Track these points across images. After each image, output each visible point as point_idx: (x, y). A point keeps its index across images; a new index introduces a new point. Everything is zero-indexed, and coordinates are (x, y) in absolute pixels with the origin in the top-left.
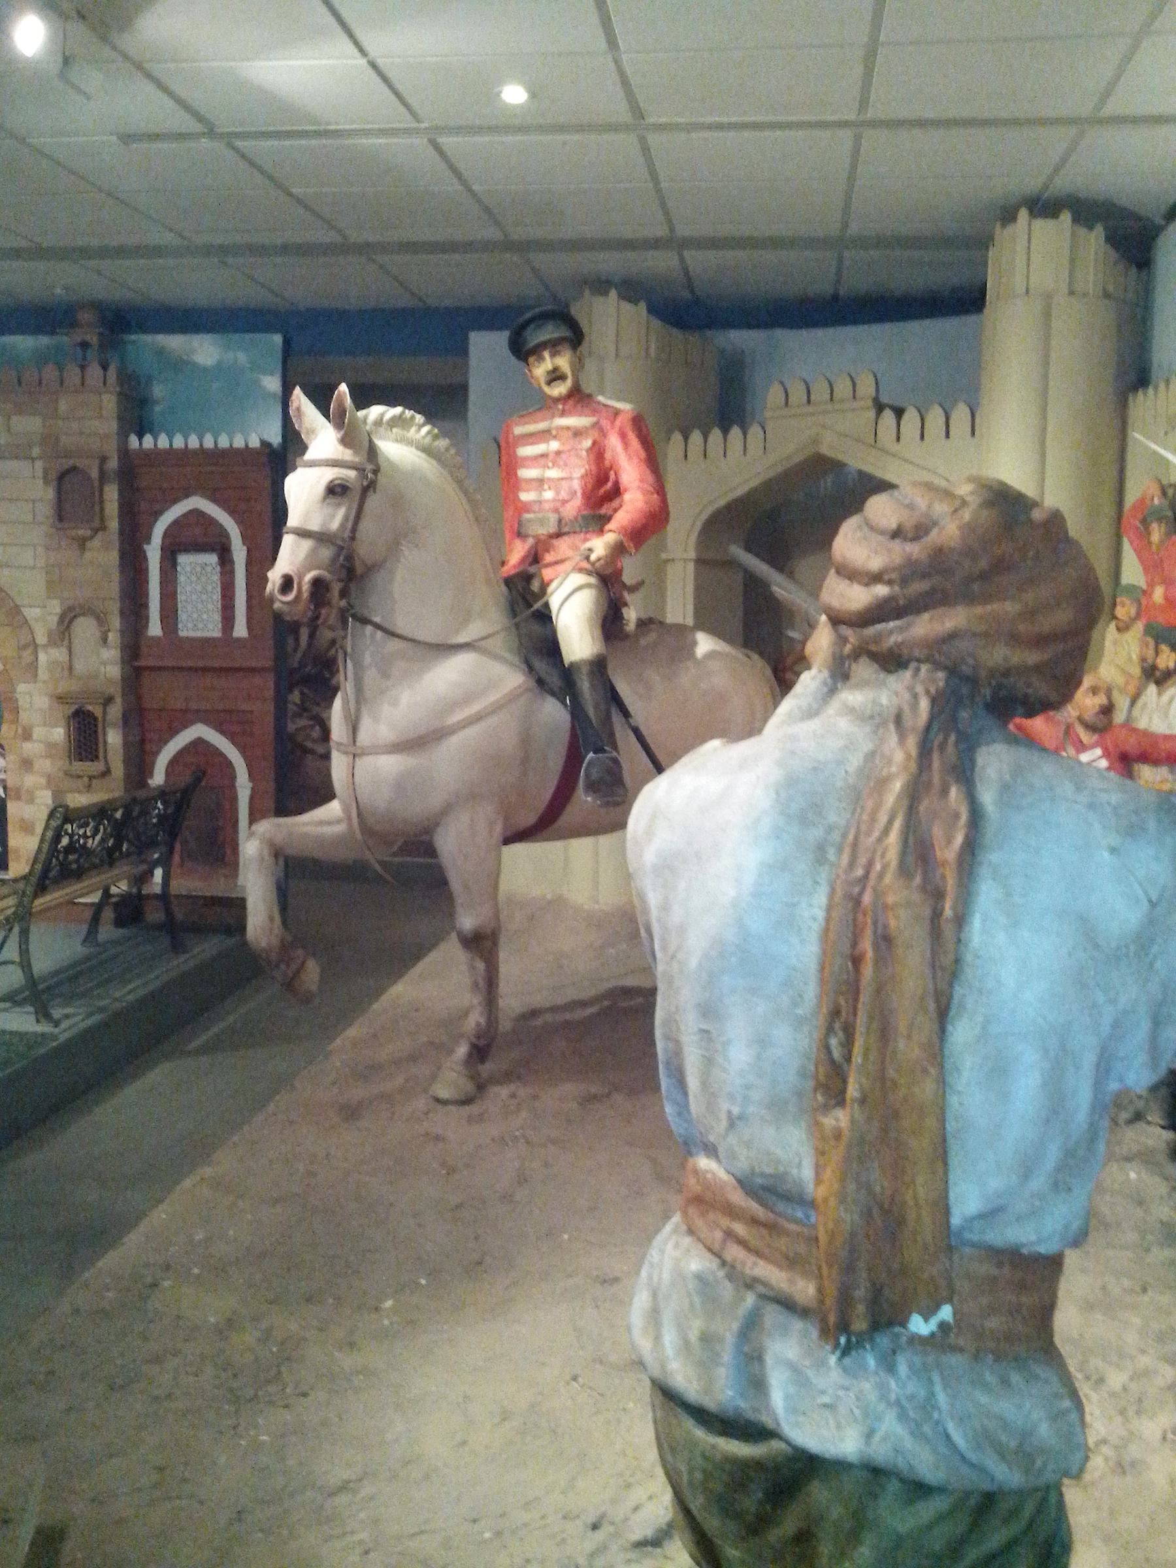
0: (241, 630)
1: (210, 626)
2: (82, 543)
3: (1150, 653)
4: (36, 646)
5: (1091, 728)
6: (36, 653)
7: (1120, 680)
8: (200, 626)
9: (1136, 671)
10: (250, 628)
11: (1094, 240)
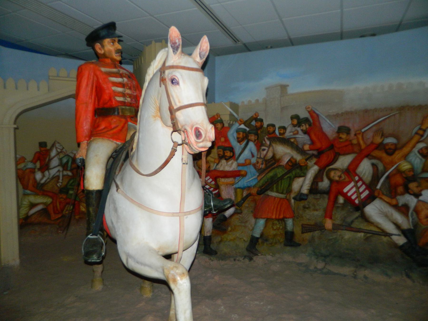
3: (221, 153)
7: (213, 160)
9: (217, 157)
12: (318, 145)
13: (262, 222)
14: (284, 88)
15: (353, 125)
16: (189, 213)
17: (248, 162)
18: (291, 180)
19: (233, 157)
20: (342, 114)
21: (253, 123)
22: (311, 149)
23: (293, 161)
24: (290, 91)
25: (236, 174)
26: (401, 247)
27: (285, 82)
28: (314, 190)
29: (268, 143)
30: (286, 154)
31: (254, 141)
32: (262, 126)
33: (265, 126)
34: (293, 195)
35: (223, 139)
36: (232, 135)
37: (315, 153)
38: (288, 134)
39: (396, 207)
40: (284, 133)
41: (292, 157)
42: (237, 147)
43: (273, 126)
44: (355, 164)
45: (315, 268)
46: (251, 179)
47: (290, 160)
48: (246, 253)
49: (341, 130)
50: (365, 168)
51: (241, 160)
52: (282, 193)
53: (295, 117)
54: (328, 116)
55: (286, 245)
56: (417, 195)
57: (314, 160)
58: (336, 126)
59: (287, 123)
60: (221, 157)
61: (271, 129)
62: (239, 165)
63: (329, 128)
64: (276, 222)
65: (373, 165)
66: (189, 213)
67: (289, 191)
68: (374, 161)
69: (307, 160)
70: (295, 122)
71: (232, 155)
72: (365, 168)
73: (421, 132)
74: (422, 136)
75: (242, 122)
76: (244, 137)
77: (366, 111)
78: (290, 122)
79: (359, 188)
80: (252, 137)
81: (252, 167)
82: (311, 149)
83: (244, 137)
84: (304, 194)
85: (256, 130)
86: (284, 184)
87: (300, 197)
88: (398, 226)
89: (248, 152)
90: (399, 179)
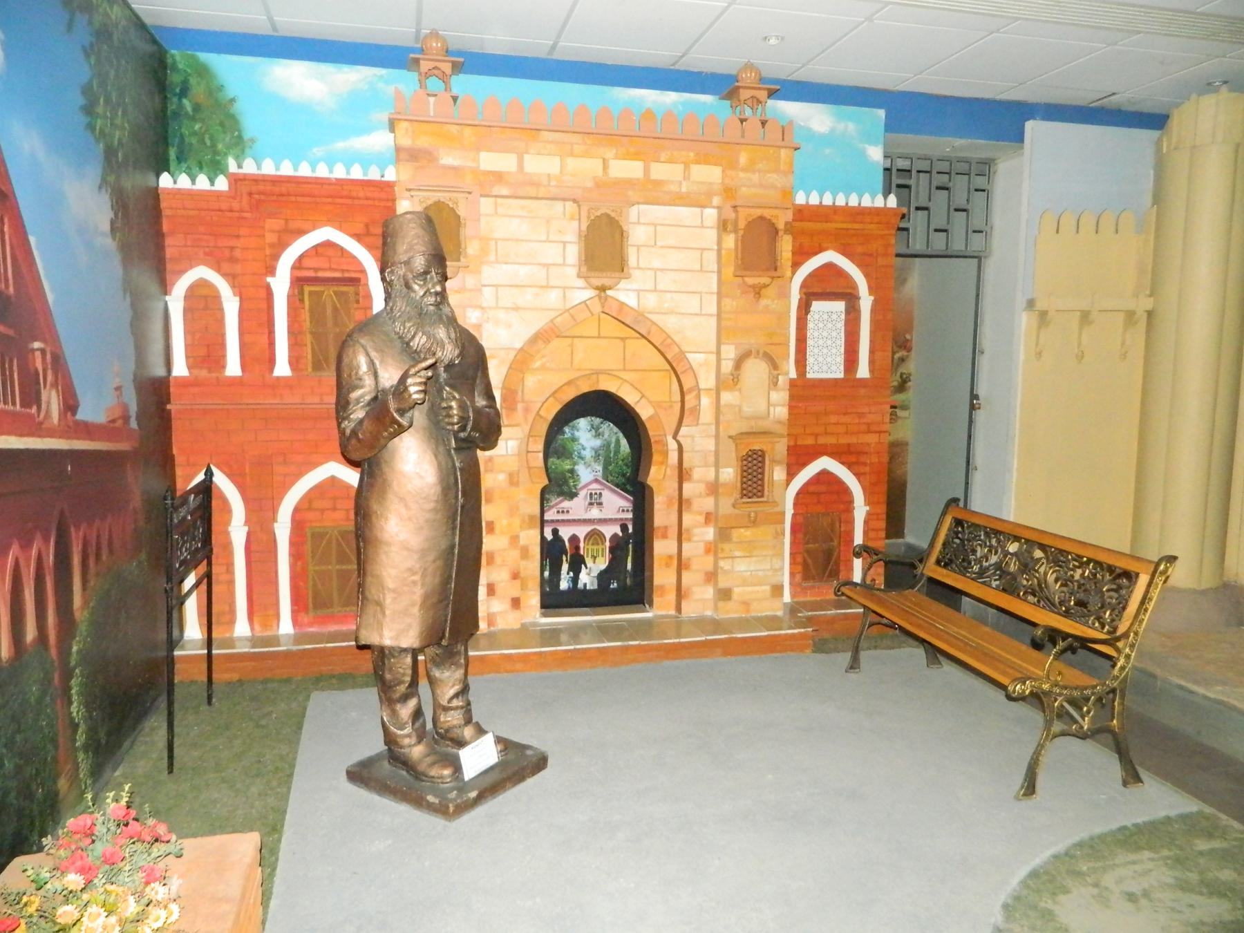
0: (863, 371)
1: (834, 368)
2: (758, 291)
4: (699, 390)
6: (698, 397)
8: (825, 368)
10: (872, 371)
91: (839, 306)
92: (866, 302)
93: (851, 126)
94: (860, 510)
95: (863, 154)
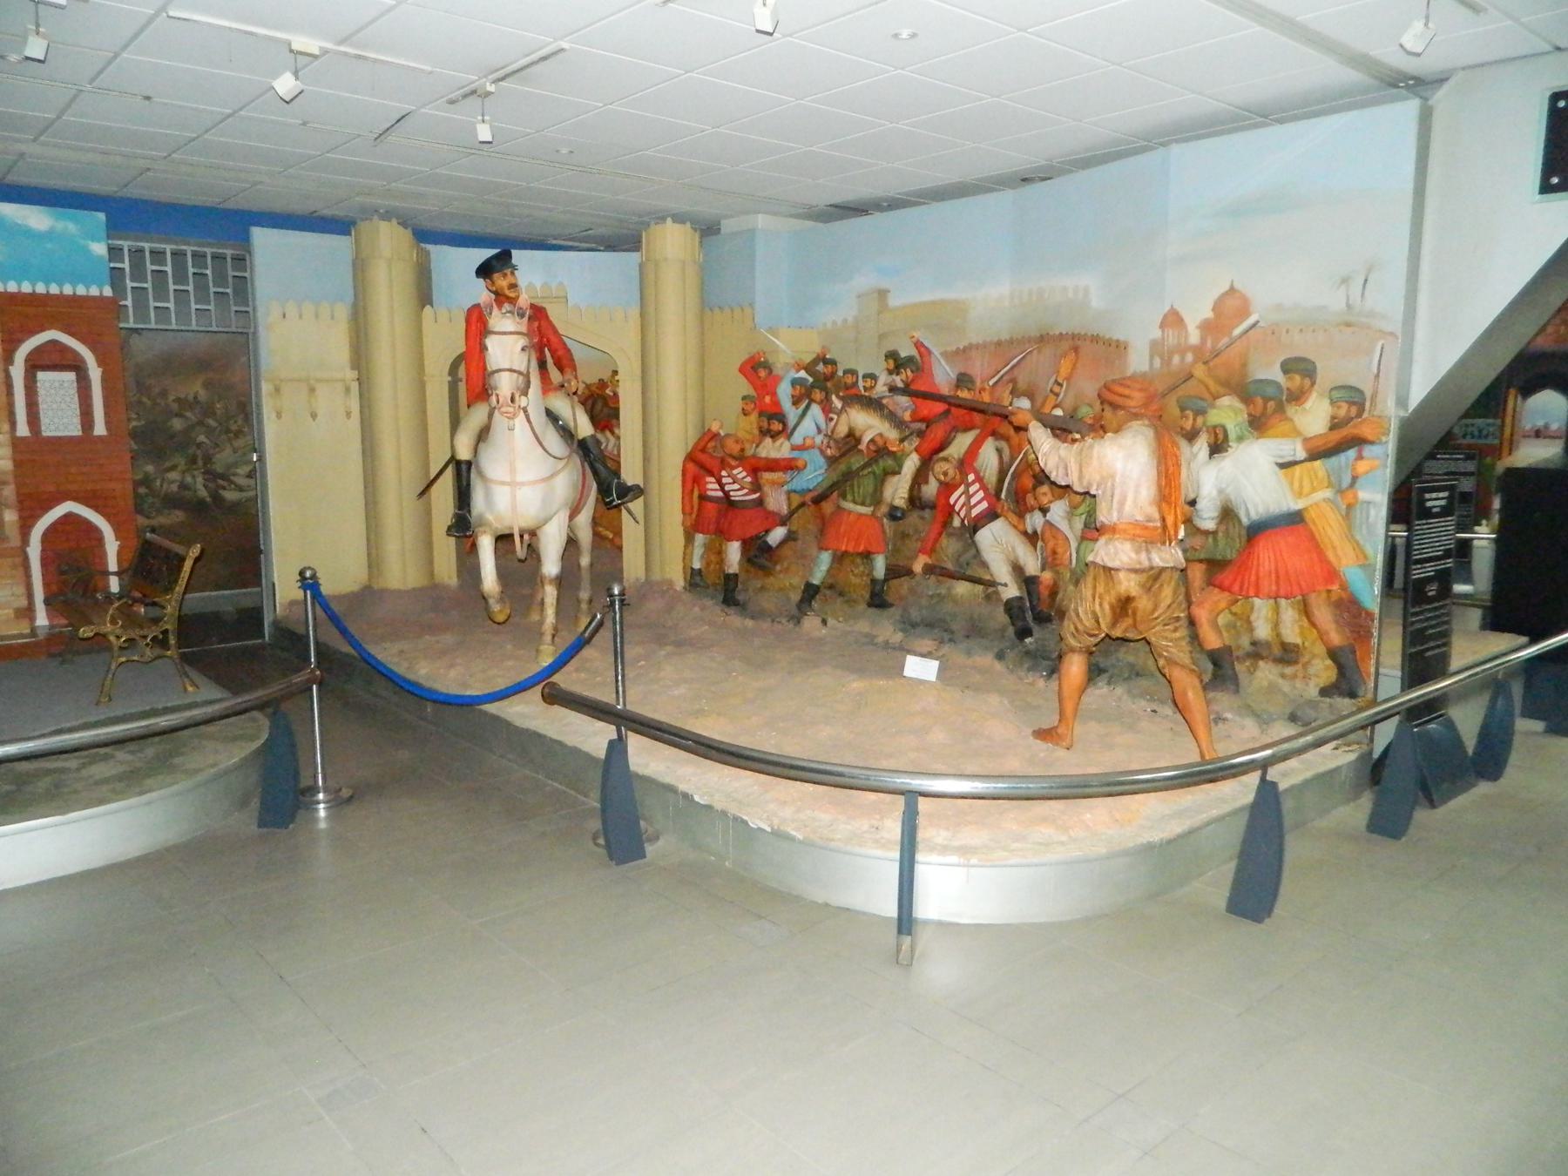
0: (100, 429)
3: (765, 425)
5: (734, 458)
9: (756, 432)
11: (697, 235)
12: (925, 412)
13: (825, 558)
14: (883, 294)
15: (978, 368)
16: (522, 484)
17: (808, 442)
18: (881, 481)
19: (786, 432)
20: (965, 350)
21: (820, 367)
22: (914, 420)
23: (880, 443)
24: (894, 301)
25: (789, 466)
26: (1011, 607)
27: (884, 285)
28: (915, 501)
29: (838, 404)
30: (870, 427)
31: (820, 403)
32: (833, 374)
33: (840, 373)
34: (884, 509)
35: (767, 399)
36: (784, 392)
37: (923, 426)
38: (881, 389)
39: (1025, 533)
40: (872, 388)
41: (881, 435)
42: (792, 413)
43: (853, 372)
44: (973, 451)
45: (887, 643)
46: (814, 474)
47: (872, 441)
48: (794, 611)
49: (963, 380)
50: (989, 458)
51: (797, 438)
52: (863, 504)
53: (892, 355)
54: (945, 354)
55: (870, 605)
56: (1044, 511)
57: (916, 442)
58: (953, 376)
59: (880, 368)
60: (765, 433)
61: (849, 380)
62: (794, 448)
63: (943, 376)
64: (859, 560)
65: (999, 451)
66: (522, 484)
67: (876, 499)
68: (1003, 445)
69: (902, 440)
70: (891, 364)
71: (780, 427)
72: (989, 458)
73: (1056, 389)
74: (1057, 395)
75: (799, 367)
76: (803, 396)
77: (999, 344)
78: (884, 365)
79: (969, 497)
80: (818, 395)
81: (817, 452)
82: (914, 420)
83: (803, 396)
84: (894, 508)
85: (826, 381)
86: (867, 485)
87: (894, 514)
88: (1017, 569)
89: (810, 425)
90: (1028, 482)
91: (70, 376)
92: (95, 373)
93: (72, 227)
94: (112, 546)
95: (87, 252)
